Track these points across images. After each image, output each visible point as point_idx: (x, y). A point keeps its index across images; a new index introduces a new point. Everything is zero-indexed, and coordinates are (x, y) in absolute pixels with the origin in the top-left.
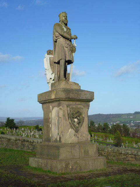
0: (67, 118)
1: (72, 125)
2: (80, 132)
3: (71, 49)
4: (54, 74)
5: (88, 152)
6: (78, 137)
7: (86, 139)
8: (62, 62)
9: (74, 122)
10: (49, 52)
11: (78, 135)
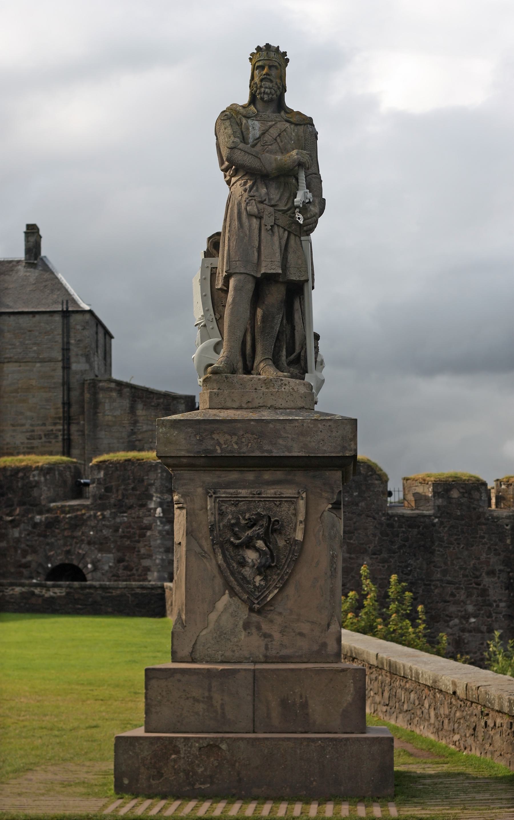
0: (207, 545)
1: (233, 581)
2: (280, 614)
5: (305, 705)
6: (266, 636)
7: (315, 647)
9: (243, 563)
11: (263, 626)
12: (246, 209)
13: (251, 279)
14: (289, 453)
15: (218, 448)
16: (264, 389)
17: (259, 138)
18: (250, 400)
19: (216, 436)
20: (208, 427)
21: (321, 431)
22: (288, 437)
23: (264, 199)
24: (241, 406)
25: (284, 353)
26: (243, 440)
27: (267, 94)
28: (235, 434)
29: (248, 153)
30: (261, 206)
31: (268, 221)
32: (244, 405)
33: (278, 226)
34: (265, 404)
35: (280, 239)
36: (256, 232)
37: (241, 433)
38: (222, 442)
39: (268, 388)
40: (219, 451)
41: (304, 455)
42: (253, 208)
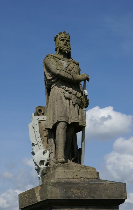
3: (79, 102)
4: (48, 152)
8: (60, 131)
10: (39, 112)
12: (64, 95)
14: (102, 197)
15: (73, 195)
16: (81, 170)
17: (67, 67)
19: (72, 190)
20: (68, 186)
21: (113, 188)
22: (100, 191)
23: (71, 92)
24: (74, 177)
26: (83, 192)
27: (67, 51)
28: (79, 189)
29: (67, 72)
31: (74, 100)
34: (83, 177)
35: (77, 108)
36: (68, 105)
37: (82, 189)
38: (74, 192)
39: (83, 170)
40: (73, 197)
41: (107, 198)
42: (67, 95)
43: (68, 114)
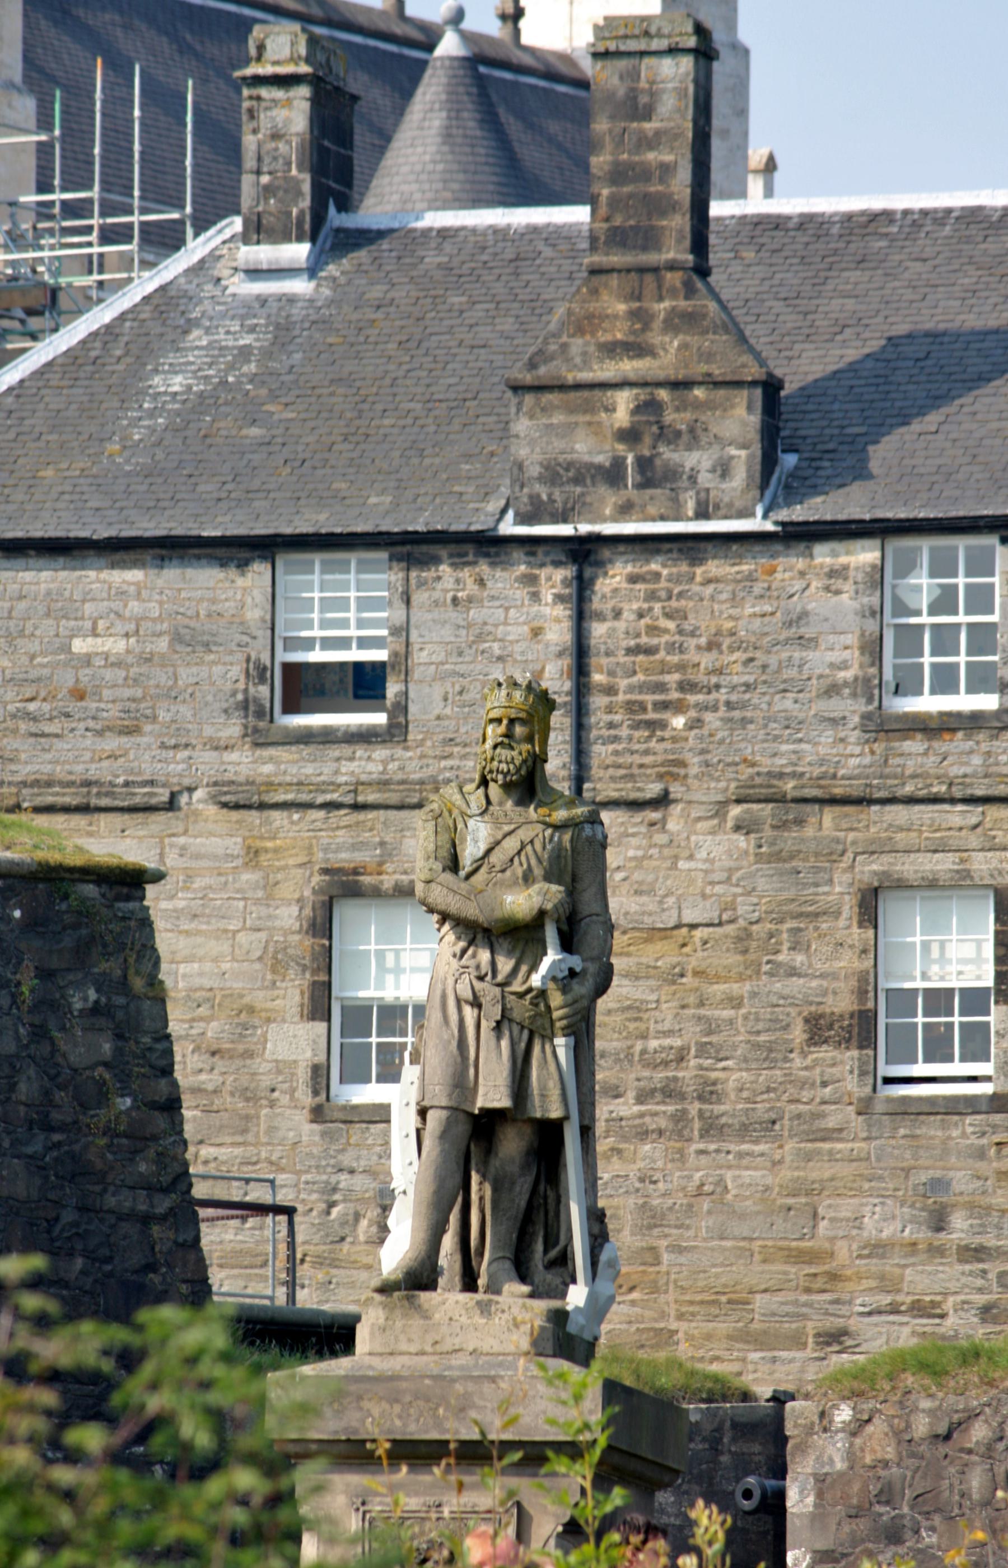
13: (462, 1117)
16: (464, 1319)
17: (483, 858)
18: (438, 1338)
19: (366, 1404)
25: (539, 1247)
28: (397, 1401)
30: (478, 985)
32: (428, 1349)
33: (510, 1020)
35: (513, 1045)
37: (408, 1398)
43: (472, 1071)
